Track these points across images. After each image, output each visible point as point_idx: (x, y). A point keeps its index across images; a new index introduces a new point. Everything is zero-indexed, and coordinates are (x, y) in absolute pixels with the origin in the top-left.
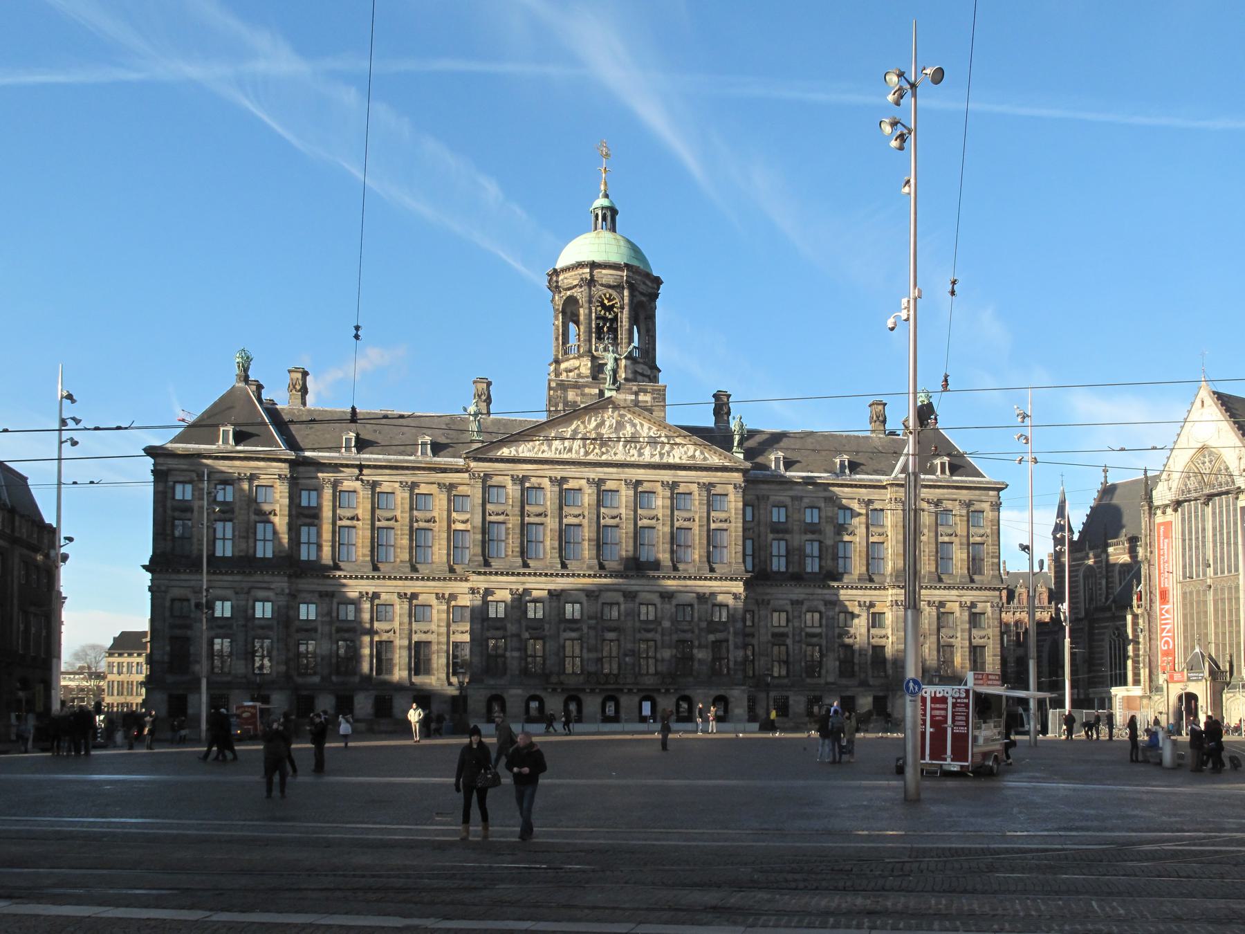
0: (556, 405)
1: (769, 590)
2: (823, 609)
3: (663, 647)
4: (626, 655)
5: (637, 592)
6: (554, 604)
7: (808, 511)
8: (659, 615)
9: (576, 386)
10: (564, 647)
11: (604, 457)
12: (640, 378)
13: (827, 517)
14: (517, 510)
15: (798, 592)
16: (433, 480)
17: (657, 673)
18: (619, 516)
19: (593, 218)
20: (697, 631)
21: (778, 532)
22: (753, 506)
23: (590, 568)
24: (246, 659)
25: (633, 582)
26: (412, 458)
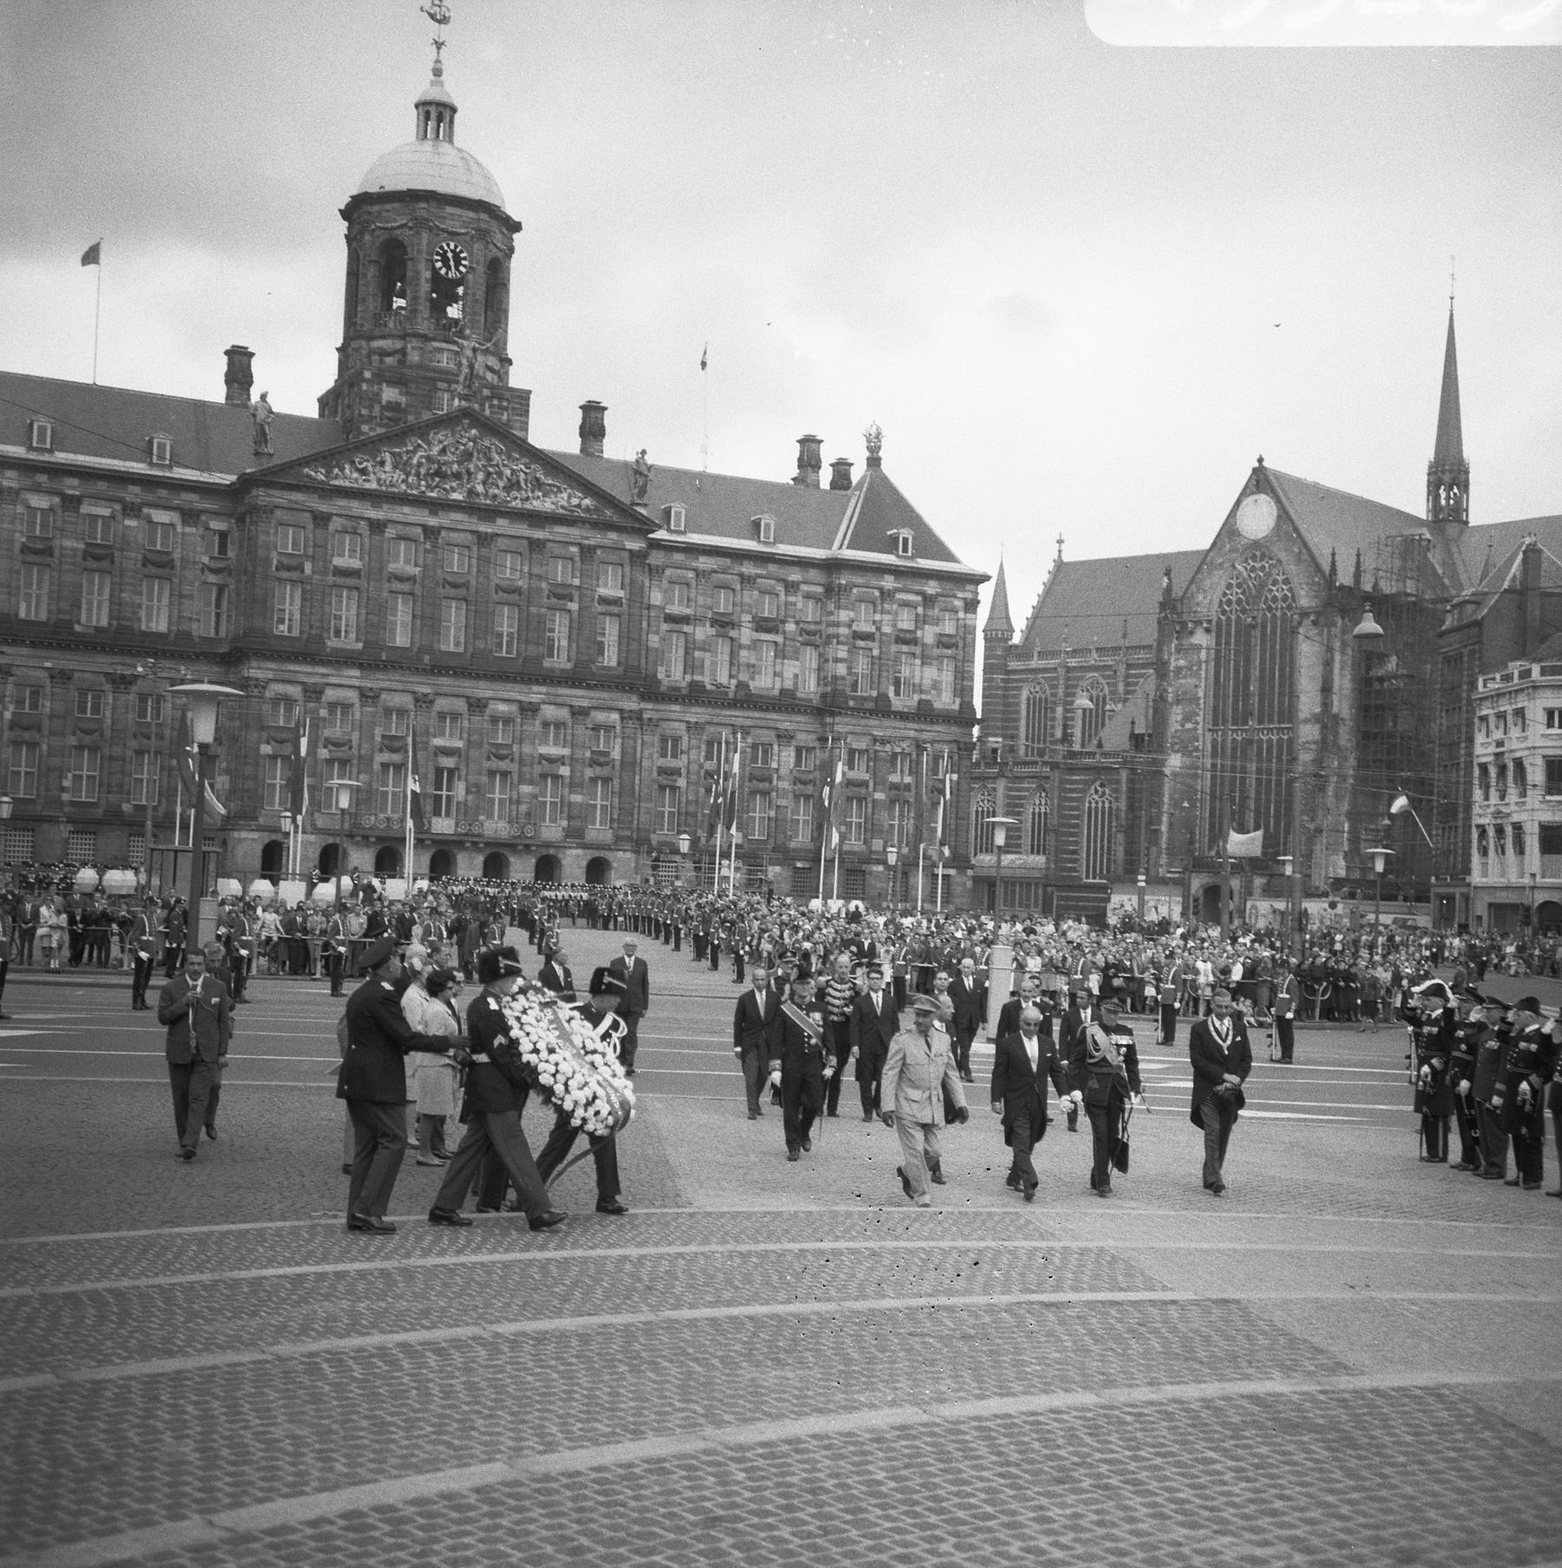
0: (371, 407)
3: (520, 783)
11: (456, 496)
12: (489, 376)
15: (697, 714)
18: (466, 585)
25: (482, 684)
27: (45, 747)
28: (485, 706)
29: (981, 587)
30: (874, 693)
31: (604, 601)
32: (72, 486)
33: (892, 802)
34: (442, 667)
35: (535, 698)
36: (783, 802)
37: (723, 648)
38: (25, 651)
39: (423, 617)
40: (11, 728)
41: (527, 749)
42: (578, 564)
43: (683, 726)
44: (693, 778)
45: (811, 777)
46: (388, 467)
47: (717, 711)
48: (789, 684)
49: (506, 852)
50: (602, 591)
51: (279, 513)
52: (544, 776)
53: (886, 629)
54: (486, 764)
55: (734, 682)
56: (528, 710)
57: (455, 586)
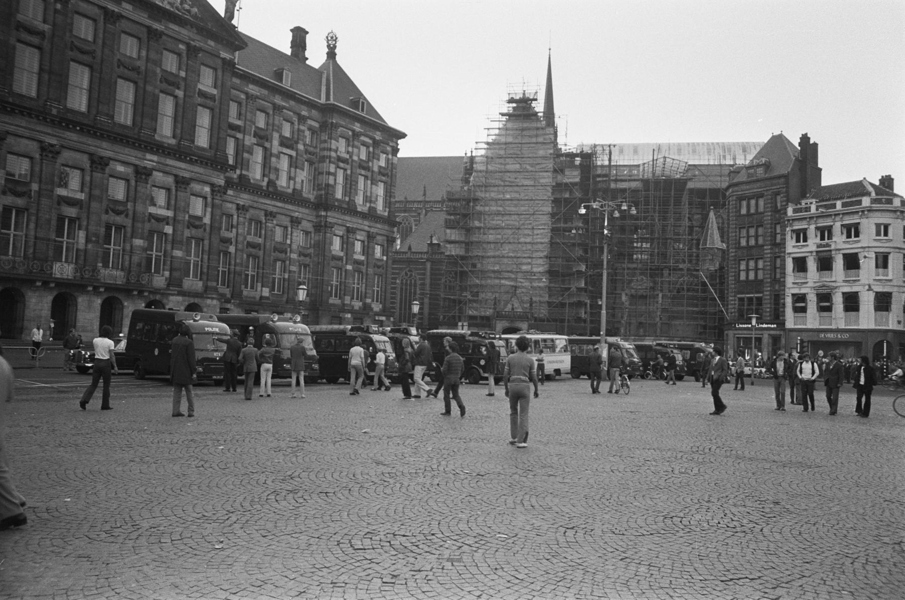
2: (263, 219)
5: (110, 159)
13: (273, 125)
15: (244, 199)
25: (105, 144)
29: (400, 141)
30: (347, 199)
31: (202, 94)
33: (355, 271)
35: (148, 164)
36: (293, 268)
37: (258, 156)
41: (140, 208)
42: (185, 59)
43: (234, 207)
47: (256, 199)
48: (298, 187)
49: (120, 296)
50: (200, 86)
52: (151, 233)
53: (355, 158)
54: (104, 217)
55: (266, 179)
56: (142, 174)
57: (83, 52)
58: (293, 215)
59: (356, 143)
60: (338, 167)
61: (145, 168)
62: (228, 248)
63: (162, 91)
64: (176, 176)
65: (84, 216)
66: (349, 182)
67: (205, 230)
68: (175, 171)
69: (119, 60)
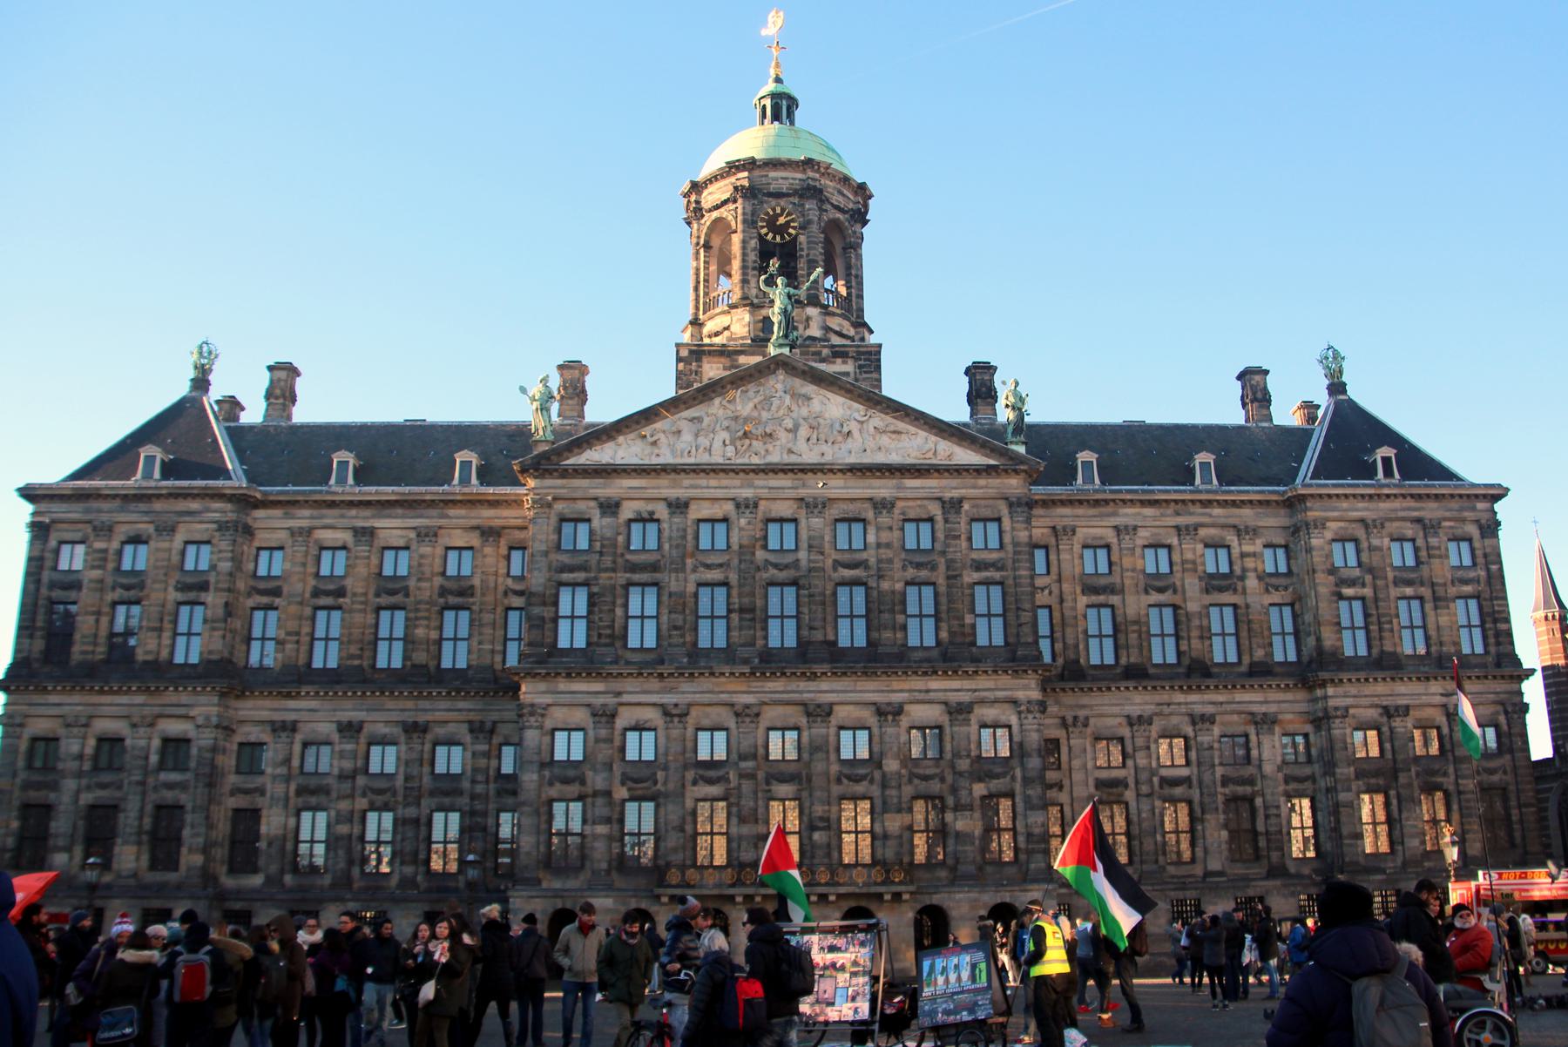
1: (1085, 700)
2: (1189, 730)
3: (885, 811)
4: (813, 828)
5: (831, 705)
6: (675, 733)
7: (1149, 553)
8: (876, 749)
9: (723, 352)
10: (694, 813)
13: (1183, 562)
14: (607, 561)
15: (1139, 701)
16: (474, 522)
17: (875, 862)
19: (758, 111)
20: (949, 778)
21: (1095, 590)
22: (1046, 547)
23: (746, 661)
24: (139, 843)
25: (824, 686)
26: (446, 487)
27: (333, 813)
28: (829, 714)
29: (1497, 507)
31: (979, 566)
32: (362, 519)
34: (770, 663)
38: (313, 704)
39: (742, 610)
40: (299, 793)
43: (1123, 721)
44: (1145, 789)
45: (1307, 771)
46: (687, 437)
47: (1164, 697)
51: (559, 506)
56: (889, 713)
58: (1255, 708)
59: (1375, 542)
60: (1341, 597)
61: (889, 704)
62: (1121, 795)
63: (908, 583)
64: (946, 703)
65: (805, 794)
66: (1374, 619)
67: (1013, 778)
68: (941, 696)
69: (835, 561)
